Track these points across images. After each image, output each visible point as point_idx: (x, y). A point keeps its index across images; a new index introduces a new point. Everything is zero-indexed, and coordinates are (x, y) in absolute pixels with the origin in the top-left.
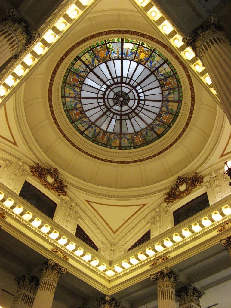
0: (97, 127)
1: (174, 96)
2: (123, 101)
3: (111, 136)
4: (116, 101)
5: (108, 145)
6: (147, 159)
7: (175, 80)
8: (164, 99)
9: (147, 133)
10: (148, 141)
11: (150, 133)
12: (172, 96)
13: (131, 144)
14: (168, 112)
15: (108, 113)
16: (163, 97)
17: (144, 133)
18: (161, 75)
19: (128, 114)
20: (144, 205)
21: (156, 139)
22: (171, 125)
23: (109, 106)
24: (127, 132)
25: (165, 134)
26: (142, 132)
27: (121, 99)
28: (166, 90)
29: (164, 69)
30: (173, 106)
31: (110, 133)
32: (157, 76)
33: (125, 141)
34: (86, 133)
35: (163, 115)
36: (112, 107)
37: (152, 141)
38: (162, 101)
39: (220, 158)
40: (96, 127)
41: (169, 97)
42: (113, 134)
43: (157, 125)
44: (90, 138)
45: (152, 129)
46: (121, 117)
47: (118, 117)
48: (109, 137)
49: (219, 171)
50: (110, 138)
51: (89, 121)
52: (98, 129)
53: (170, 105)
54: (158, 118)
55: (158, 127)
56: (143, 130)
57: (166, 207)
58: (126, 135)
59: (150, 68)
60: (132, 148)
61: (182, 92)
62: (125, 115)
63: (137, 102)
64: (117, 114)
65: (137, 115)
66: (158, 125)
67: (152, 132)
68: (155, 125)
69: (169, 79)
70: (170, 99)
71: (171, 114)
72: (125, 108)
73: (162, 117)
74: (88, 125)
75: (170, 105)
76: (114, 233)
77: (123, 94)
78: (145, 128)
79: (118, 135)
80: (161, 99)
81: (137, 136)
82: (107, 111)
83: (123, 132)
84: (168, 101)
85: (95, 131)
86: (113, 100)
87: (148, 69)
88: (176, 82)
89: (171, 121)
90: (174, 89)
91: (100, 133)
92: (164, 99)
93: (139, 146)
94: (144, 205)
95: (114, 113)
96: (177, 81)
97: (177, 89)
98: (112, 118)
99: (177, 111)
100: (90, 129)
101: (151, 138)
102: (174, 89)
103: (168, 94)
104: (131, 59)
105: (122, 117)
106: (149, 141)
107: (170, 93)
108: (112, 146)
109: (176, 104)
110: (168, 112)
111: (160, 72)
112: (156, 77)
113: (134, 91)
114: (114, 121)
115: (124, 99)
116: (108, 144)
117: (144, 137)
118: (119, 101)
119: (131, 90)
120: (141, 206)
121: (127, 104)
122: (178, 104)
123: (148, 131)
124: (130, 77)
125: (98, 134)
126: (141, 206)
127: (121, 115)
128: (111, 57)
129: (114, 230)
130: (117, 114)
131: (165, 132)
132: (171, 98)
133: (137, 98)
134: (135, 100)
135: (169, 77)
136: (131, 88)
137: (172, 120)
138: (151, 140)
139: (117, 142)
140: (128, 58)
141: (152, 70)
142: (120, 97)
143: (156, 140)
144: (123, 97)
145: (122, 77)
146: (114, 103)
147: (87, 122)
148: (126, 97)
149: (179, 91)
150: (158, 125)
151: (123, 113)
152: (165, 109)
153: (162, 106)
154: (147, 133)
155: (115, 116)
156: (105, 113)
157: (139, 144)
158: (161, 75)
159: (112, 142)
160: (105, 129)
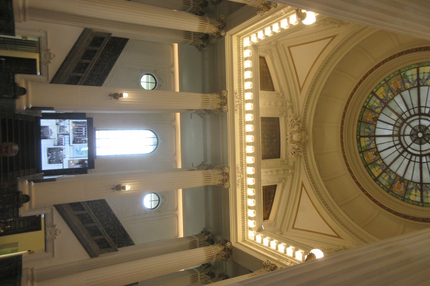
0: (411, 88)
1: (385, 180)
2: (417, 135)
3: (392, 94)
4: (422, 128)
5: (384, 84)
6: (344, 114)
7: (398, 194)
8: (389, 170)
9: (370, 129)
10: (362, 124)
11: (367, 132)
12: (387, 178)
13: (369, 106)
14: (374, 163)
15: (416, 110)
16: (391, 170)
17: (371, 127)
18: (412, 188)
19: (400, 128)
20: (301, 90)
21: (359, 131)
22: (361, 155)
23: (423, 117)
24: (383, 112)
25: (358, 143)
26: (373, 126)
27: (420, 135)
28: (395, 179)
29: (416, 195)
30: (376, 171)
31: (395, 96)
32: (415, 184)
33: (377, 103)
34: (414, 71)
36: (420, 119)
37: (359, 127)
38: (388, 167)
39: (302, 182)
40: (412, 86)
41: (387, 175)
42: (391, 97)
43: (370, 144)
44: (406, 71)
45: (369, 136)
46: (402, 119)
47: (404, 117)
48: (392, 92)
49: (291, 176)
50: (390, 91)
51: (425, 84)
52: (409, 87)
53: (379, 169)
54: (375, 150)
55: (367, 143)
56: (374, 128)
57: (287, 114)
58: (381, 108)
59: (428, 185)
60: (365, 104)
62: (402, 125)
63: (406, 146)
64: (408, 118)
65: (393, 136)
66: (369, 145)
67: (367, 134)
68: (372, 142)
69: (403, 190)
70: (384, 174)
71: (371, 164)
72: (408, 130)
73: (375, 154)
74: (421, 79)
75: (379, 169)
76: (289, 48)
77: (424, 141)
78: (375, 131)
79: (386, 102)
80: (391, 168)
81: (373, 118)
82: (420, 110)
83: (386, 108)
84: (384, 171)
85: (409, 82)
86: (425, 126)
88: (396, 192)
89: (365, 158)
90: (391, 185)
91: (403, 86)
92: (389, 170)
93: (362, 112)
94: (301, 90)
95: (411, 116)
96: (396, 194)
97: (389, 188)
98: (408, 110)
99: (370, 170)
100: (415, 78)
101: (362, 129)
102: (391, 185)
103: (390, 177)
105: (402, 121)
106: (360, 125)
107: (391, 180)
108: (380, 87)
109: (376, 175)
110: (374, 163)
111: (416, 190)
112: (415, 183)
113: (419, 153)
114: (404, 109)
115: (418, 138)
116: (385, 84)
117: (368, 123)
118: (420, 132)
119: (421, 151)
120: (301, 86)
121: (411, 135)
122: (375, 176)
123: (370, 132)
125: (403, 83)
126: (301, 86)
127: (404, 121)
129: (291, 48)
130: (408, 118)
131: (359, 145)
132: (386, 176)
133: (409, 149)
134: (409, 146)
135: (405, 192)
137: (366, 159)
138: (360, 127)
139: (381, 95)
141: (424, 185)
142: (424, 136)
143: (357, 131)
144: (420, 138)
146: (423, 126)
147: (426, 81)
148: (418, 141)
149: (386, 187)
150: (369, 145)
151: (405, 124)
152: (379, 162)
153: (384, 162)
154: (370, 129)
155: (408, 115)
156: (419, 107)
157: (364, 114)
158: (412, 188)
159: (385, 89)
160: (402, 93)
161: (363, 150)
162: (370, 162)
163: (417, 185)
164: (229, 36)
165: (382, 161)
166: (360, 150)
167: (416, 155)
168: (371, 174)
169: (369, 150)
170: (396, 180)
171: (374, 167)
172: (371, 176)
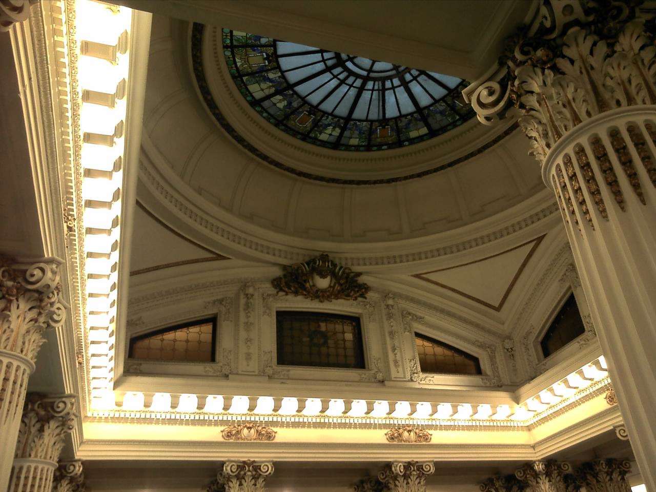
14: (259, 74)
22: (228, 53)
35: (265, 63)
41: (283, 100)
59: (358, 123)
61: (268, 119)
69: (309, 126)
70: (279, 97)
71: (252, 74)
87: (360, 121)
92: (291, 92)
99: (245, 85)
104: (403, 119)
107: (290, 108)
110: (259, 74)
124: (387, 92)
128: (444, 104)
136: (372, 75)
137: (239, 64)
140: (409, 117)
145: (405, 85)
158: (329, 125)
161: (235, 43)
162: (250, 70)
163: (339, 120)
164: (537, 449)
165: (280, 74)
166: (228, 41)
167: (357, 76)
168: (246, 93)
169: (253, 47)
170: (301, 110)
171: (258, 82)
172: (245, 96)
